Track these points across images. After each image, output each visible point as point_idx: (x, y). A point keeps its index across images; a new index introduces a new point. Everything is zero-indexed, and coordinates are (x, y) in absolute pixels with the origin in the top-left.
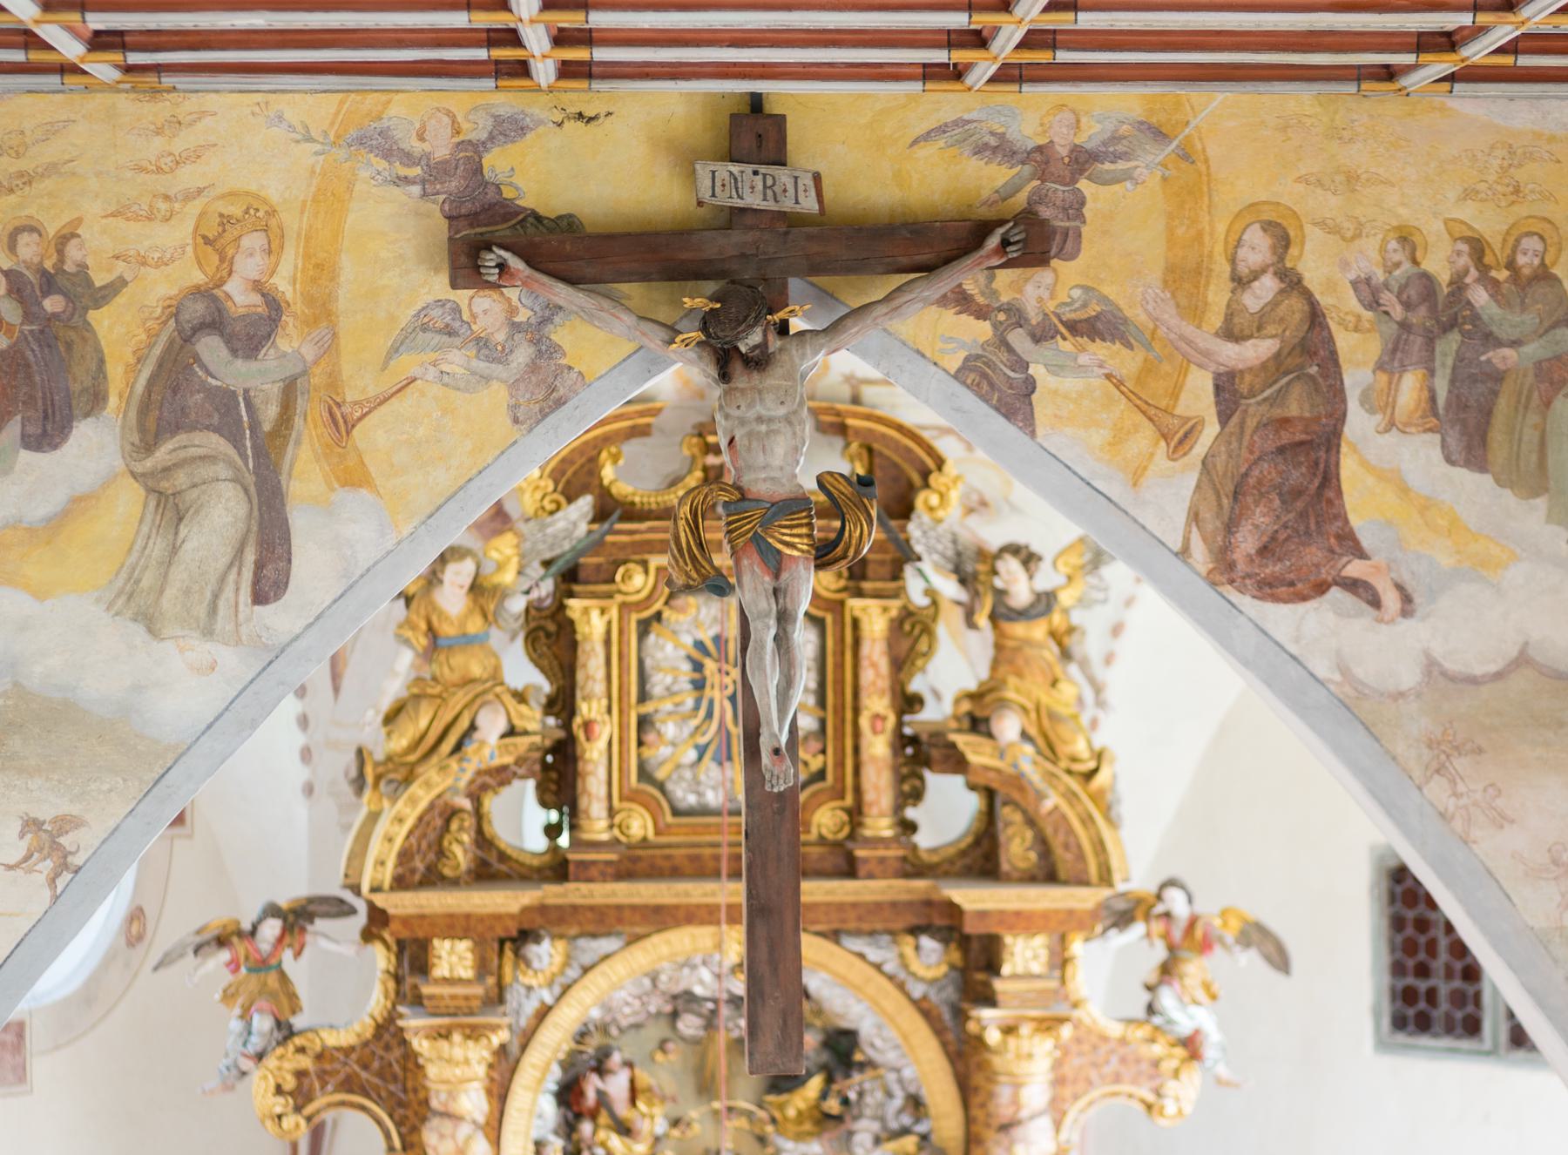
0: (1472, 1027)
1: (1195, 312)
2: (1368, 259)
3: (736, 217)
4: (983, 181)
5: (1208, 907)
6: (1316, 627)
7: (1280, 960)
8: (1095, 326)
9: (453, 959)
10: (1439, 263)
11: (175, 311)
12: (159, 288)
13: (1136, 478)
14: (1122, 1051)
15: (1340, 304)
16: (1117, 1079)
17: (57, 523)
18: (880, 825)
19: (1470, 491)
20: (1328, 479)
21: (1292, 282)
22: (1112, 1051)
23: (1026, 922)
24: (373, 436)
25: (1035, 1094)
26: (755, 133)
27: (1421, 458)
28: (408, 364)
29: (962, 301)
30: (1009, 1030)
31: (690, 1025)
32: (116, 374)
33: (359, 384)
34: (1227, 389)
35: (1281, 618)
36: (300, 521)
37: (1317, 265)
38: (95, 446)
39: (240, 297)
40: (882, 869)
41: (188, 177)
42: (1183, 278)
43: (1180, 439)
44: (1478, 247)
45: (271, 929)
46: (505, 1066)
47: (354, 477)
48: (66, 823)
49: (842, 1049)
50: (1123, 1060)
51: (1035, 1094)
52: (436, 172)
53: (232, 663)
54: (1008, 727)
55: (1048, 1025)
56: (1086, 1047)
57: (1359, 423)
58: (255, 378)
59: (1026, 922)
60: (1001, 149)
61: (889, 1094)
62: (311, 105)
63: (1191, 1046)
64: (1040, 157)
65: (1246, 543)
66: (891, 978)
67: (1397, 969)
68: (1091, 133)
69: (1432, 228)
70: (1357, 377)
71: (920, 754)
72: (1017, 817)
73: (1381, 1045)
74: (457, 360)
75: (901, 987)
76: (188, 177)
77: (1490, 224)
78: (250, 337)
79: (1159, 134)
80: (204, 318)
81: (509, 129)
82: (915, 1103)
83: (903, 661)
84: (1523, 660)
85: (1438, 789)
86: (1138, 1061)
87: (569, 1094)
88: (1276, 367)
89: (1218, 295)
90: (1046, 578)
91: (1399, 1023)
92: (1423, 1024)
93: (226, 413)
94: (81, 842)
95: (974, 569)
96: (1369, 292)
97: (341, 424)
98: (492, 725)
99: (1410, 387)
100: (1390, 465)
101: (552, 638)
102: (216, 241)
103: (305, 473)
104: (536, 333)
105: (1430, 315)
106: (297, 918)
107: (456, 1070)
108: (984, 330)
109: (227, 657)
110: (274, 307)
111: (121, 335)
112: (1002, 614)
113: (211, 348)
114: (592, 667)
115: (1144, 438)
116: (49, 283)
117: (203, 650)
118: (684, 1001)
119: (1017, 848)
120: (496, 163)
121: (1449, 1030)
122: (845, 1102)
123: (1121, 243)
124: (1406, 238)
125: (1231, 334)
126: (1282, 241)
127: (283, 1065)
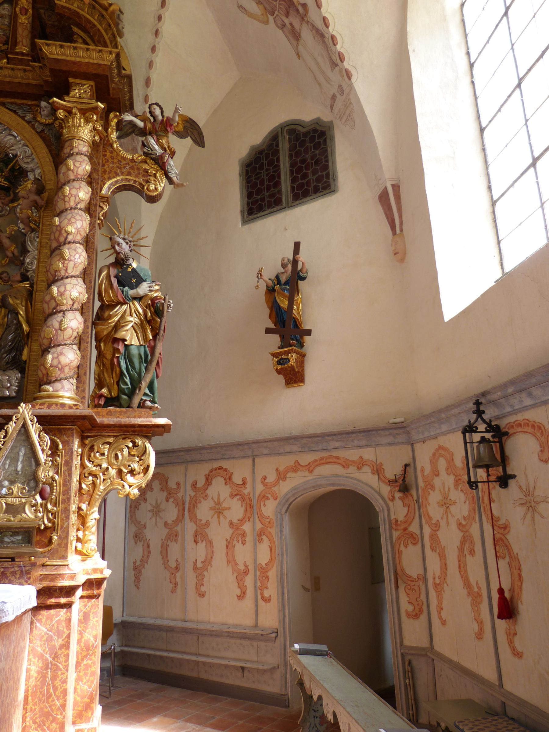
7: (199, 141)
14: (131, 164)
16: (129, 174)
22: (128, 164)
50: (132, 168)
56: (115, 161)
66: (29, 123)
67: (250, 196)
73: (245, 222)
75: (33, 127)
86: (138, 169)
92: (260, 209)
121: (270, 206)
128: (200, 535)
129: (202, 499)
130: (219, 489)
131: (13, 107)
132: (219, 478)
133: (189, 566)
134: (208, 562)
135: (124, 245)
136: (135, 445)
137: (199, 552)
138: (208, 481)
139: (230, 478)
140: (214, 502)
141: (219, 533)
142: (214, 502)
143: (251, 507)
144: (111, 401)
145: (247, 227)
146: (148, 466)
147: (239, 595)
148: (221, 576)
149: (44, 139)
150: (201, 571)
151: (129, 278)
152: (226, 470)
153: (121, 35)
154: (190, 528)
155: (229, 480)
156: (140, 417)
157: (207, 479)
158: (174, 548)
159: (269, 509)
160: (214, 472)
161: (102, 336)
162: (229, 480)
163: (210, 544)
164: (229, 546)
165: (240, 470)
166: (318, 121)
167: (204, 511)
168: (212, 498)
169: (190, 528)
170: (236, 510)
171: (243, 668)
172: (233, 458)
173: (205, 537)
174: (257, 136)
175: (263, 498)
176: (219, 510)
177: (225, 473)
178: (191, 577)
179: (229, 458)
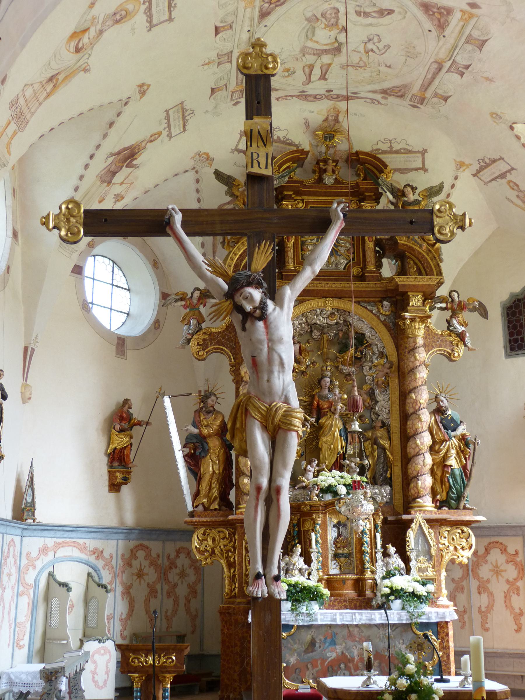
5: (464, 298)
14: (441, 338)
16: (440, 346)
18: (372, 267)
22: (439, 338)
25: (420, 341)
30: (413, 320)
31: (316, 334)
40: (373, 278)
45: (197, 294)
49: (361, 339)
50: (442, 341)
56: (431, 337)
59: (416, 289)
61: (374, 353)
66: (375, 315)
67: (511, 334)
72: (412, 262)
73: (507, 356)
75: (378, 317)
82: (382, 355)
86: (446, 341)
90: (416, 197)
91: (512, 349)
122: (362, 353)
127: (199, 337)
128: (482, 588)
129: (483, 564)
131: (365, 305)
132: (496, 549)
133: (475, 610)
134: (490, 607)
135: (446, 402)
136: (463, 531)
137: (484, 600)
139: (505, 550)
140: (493, 566)
141: (498, 588)
142: (493, 566)
145: (510, 360)
146: (472, 545)
147: (516, 629)
149: (385, 325)
151: (450, 425)
152: (501, 544)
153: (441, 261)
154: (474, 584)
155: (504, 550)
156: (465, 515)
157: (486, 549)
160: (492, 545)
162: (504, 550)
164: (507, 596)
167: (485, 572)
168: (491, 563)
169: (474, 584)
170: (511, 572)
171: (522, 676)
172: (507, 536)
173: (487, 590)
176: (497, 571)
177: (501, 546)
178: (477, 618)
179: (504, 536)
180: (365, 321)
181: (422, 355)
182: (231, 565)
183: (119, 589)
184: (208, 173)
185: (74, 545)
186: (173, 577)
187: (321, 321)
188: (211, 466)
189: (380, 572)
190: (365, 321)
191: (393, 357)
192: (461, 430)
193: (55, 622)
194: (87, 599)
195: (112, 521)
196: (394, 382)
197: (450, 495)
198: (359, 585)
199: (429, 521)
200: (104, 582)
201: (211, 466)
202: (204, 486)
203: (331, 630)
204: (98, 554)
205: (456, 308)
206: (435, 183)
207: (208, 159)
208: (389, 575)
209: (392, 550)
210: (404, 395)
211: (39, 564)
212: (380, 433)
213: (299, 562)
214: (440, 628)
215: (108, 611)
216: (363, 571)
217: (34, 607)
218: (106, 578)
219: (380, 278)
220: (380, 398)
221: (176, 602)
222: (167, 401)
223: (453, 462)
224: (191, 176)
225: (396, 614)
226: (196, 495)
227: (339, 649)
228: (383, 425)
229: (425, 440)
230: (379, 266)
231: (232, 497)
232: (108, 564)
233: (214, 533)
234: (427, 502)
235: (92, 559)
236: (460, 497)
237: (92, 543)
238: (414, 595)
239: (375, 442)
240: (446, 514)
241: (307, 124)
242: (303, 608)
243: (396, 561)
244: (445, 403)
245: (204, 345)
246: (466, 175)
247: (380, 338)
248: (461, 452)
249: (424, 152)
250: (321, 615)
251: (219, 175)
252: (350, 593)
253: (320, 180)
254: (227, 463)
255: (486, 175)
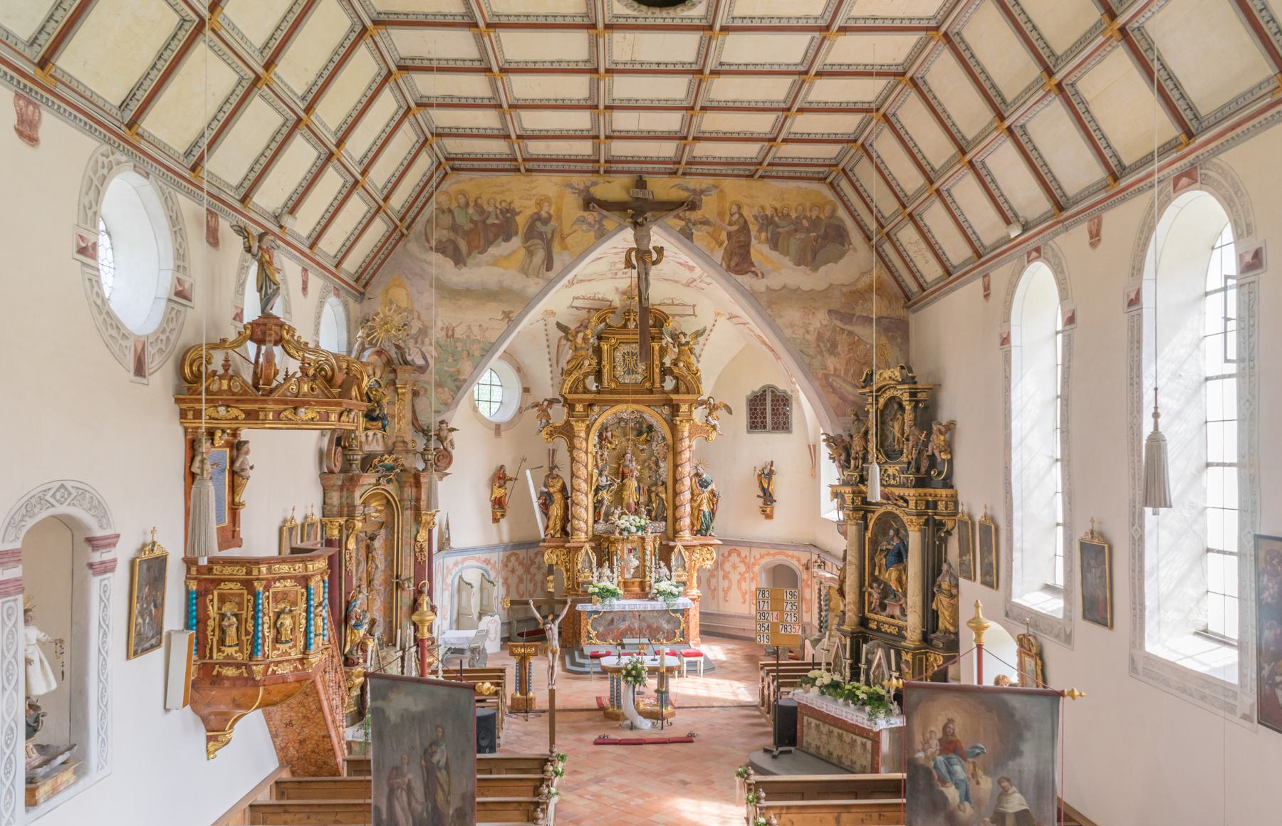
0: (765, 427)
1: (723, 221)
2: (755, 211)
3: (637, 199)
4: (683, 195)
5: (717, 402)
6: (745, 280)
7: (730, 412)
8: (705, 222)
9: (579, 407)
10: (769, 212)
11: (531, 217)
12: (529, 212)
13: (712, 251)
15: (750, 219)
17: (510, 255)
18: (657, 385)
19: (774, 254)
20: (748, 253)
21: (741, 215)
23: (684, 401)
24: (569, 240)
25: (686, 434)
26: (641, 184)
27: (765, 249)
28: (575, 227)
29: (680, 218)
31: (622, 424)
32: (520, 228)
33: (566, 231)
34: (729, 235)
35: (740, 278)
36: (555, 256)
37: (745, 212)
38: (516, 242)
39: (544, 214)
40: (657, 393)
41: (534, 192)
42: (721, 214)
43: (721, 244)
44: (776, 209)
46: (589, 429)
47: (565, 248)
48: (511, 312)
51: (686, 434)
52: (580, 192)
53: (542, 282)
54: (681, 364)
55: (688, 421)
57: (754, 242)
58: (547, 230)
59: (684, 401)
60: (687, 189)
62: (557, 178)
63: (714, 427)
64: (694, 191)
65: (733, 264)
68: (704, 186)
69: (767, 206)
70: (753, 233)
71: (665, 372)
74: (585, 227)
76: (534, 192)
77: (778, 205)
78: (546, 221)
79: (716, 187)
80: (536, 218)
81: (595, 184)
82: (664, 438)
83: (661, 357)
84: (784, 287)
85: (769, 311)
87: (600, 436)
88: (738, 231)
89: (727, 217)
93: (541, 236)
94: (514, 316)
95: (675, 337)
96: (756, 217)
97: (563, 239)
98: (587, 363)
99: (763, 235)
100: (760, 250)
101: (598, 351)
102: (539, 204)
103: (556, 247)
104: (600, 222)
105: (767, 222)
106: (551, 402)
107: (580, 428)
108: (683, 223)
109: (541, 281)
110: (550, 216)
111: (521, 221)
112: (680, 345)
113: (538, 224)
114: (605, 355)
115: (713, 244)
116: (508, 211)
117: (537, 280)
118: (621, 419)
119: (683, 388)
120: (592, 190)
123: (709, 207)
124: (762, 207)
125: (730, 224)
126: (739, 208)
127: (548, 429)
130: (734, 558)
134: (729, 588)
137: (726, 583)
138: (730, 554)
141: (735, 577)
143: (748, 567)
144: (699, 532)
148: (735, 594)
150: (726, 592)
151: (704, 484)
154: (721, 573)
155: (739, 555)
158: (713, 581)
159: (756, 569)
161: (696, 511)
162: (739, 555)
163: (730, 581)
165: (744, 551)
166: (785, 392)
167: (727, 566)
169: (721, 573)
170: (742, 568)
174: (757, 387)
175: (754, 564)
176: (734, 567)
178: (721, 594)
180: (654, 417)
181: (686, 443)
182: (567, 570)
183: (501, 581)
184: (552, 321)
185: (473, 558)
186: (533, 570)
187: (625, 416)
188: (556, 510)
189: (653, 580)
190: (654, 417)
191: (670, 441)
192: (710, 488)
193: (464, 603)
194: (482, 590)
195: (495, 541)
196: (670, 457)
197: (702, 529)
198: (642, 585)
199: (686, 547)
200: (491, 579)
201: (556, 510)
202: (551, 523)
203: (623, 615)
204: (488, 562)
205: (713, 408)
206: (700, 328)
207: (553, 313)
208: (658, 581)
209: (662, 564)
210: (676, 466)
211: (454, 572)
212: (661, 489)
213: (606, 571)
214: (684, 612)
215: (495, 594)
216: (645, 577)
217: (452, 596)
218: (493, 575)
219: (663, 392)
220: (662, 465)
221: (535, 585)
222: (528, 472)
223: (705, 508)
224: (542, 322)
225: (659, 604)
226: (547, 528)
227: (627, 623)
228: (663, 483)
229: (687, 496)
230: (663, 381)
231: (569, 529)
232: (494, 567)
233: (557, 552)
234: (686, 535)
235: (484, 566)
236: (707, 529)
237: (483, 556)
238: (671, 593)
239: (657, 495)
240: (699, 540)
241: (617, 289)
242: (607, 602)
243: (665, 570)
244: (701, 471)
245: (551, 435)
246: (722, 321)
247: (662, 428)
248: (710, 500)
249: (694, 306)
250: (618, 604)
251: (559, 325)
252: (637, 589)
253: (625, 326)
254: (566, 508)
255: (734, 320)
